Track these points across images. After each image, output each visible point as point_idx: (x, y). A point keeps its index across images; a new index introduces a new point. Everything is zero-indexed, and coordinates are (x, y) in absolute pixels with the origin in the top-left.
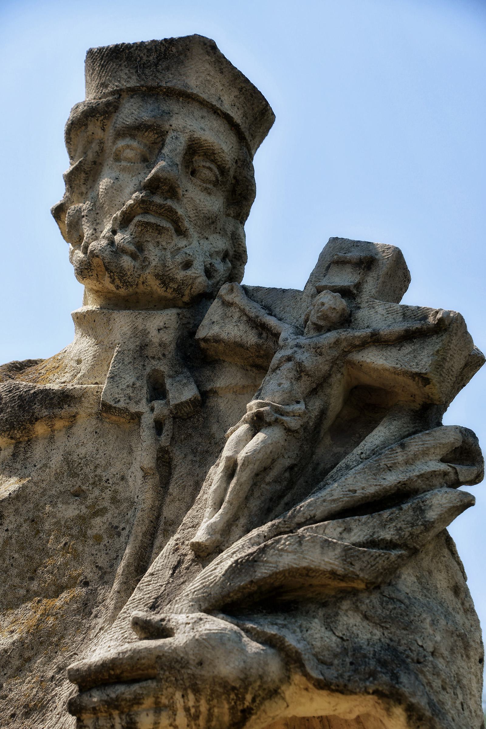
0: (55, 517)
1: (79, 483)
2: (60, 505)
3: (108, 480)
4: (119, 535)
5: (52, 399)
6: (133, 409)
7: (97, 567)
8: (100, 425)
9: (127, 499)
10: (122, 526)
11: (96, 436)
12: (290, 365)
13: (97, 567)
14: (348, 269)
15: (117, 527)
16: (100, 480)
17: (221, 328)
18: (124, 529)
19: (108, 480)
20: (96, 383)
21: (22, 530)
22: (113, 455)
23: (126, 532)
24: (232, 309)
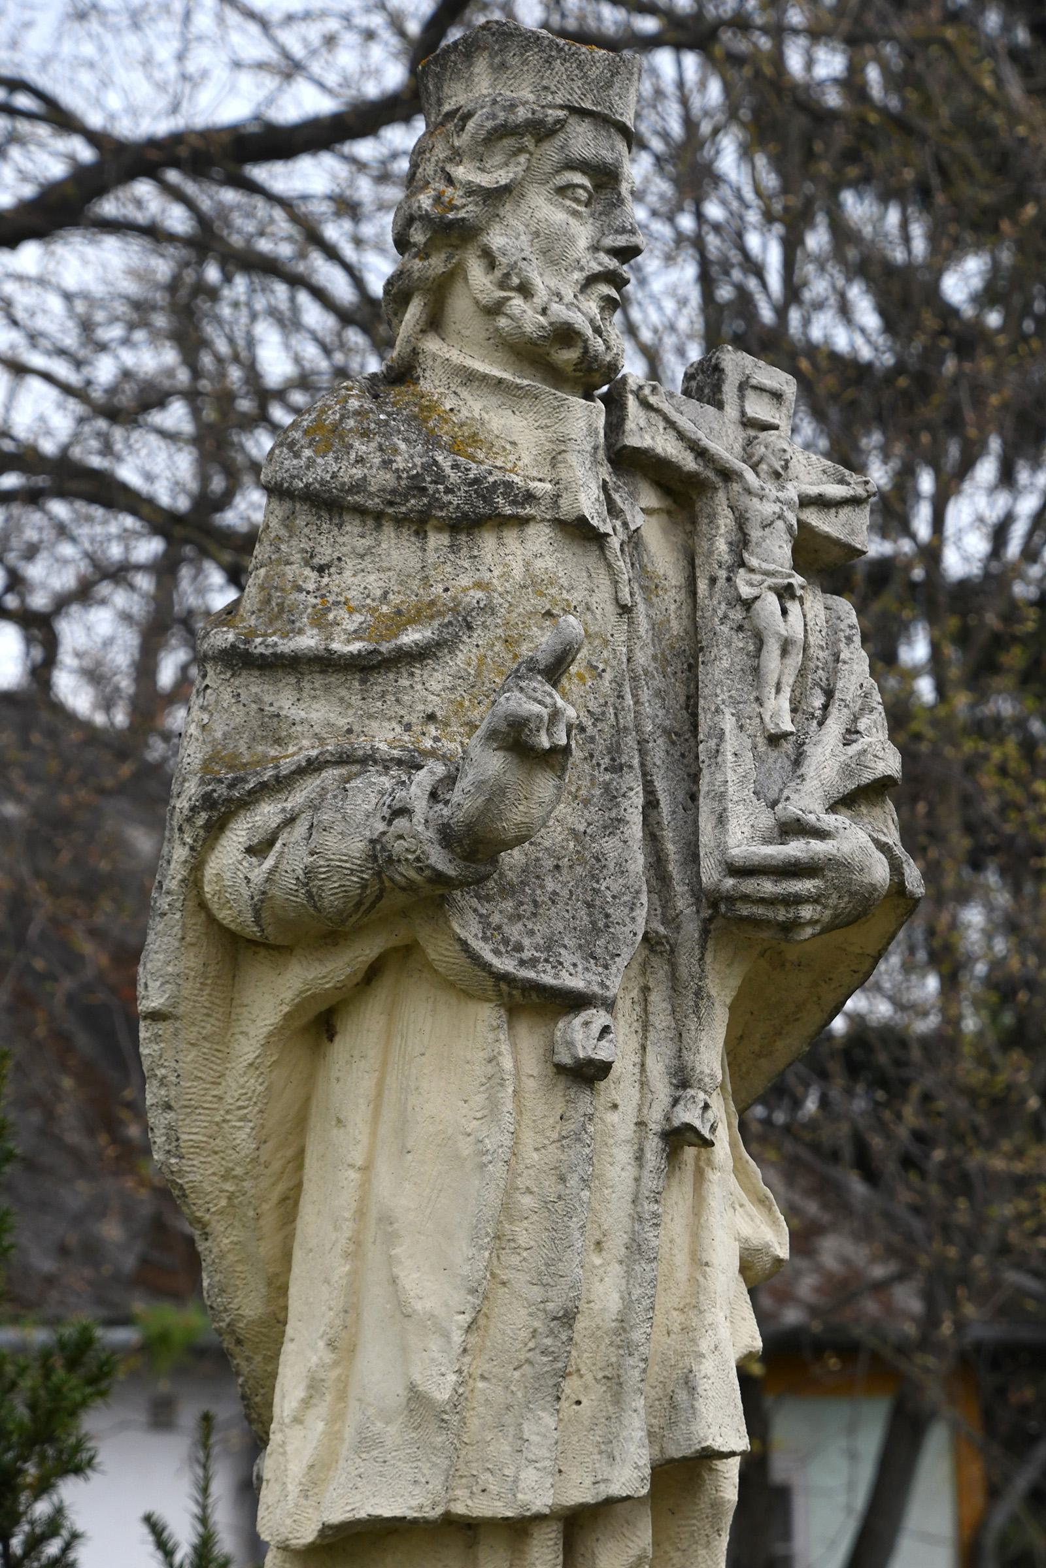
0: (532, 642)
1: (548, 607)
2: (535, 629)
3: (575, 607)
4: (600, 676)
5: (516, 495)
6: (602, 530)
7: (589, 711)
8: (552, 535)
9: (596, 633)
10: (601, 666)
11: (551, 548)
12: (780, 524)
13: (589, 711)
14: (766, 398)
15: (596, 668)
16: (569, 606)
17: (653, 438)
18: (604, 671)
19: (575, 607)
20: (540, 480)
21: (496, 649)
22: (574, 576)
23: (608, 676)
24: (653, 414)
